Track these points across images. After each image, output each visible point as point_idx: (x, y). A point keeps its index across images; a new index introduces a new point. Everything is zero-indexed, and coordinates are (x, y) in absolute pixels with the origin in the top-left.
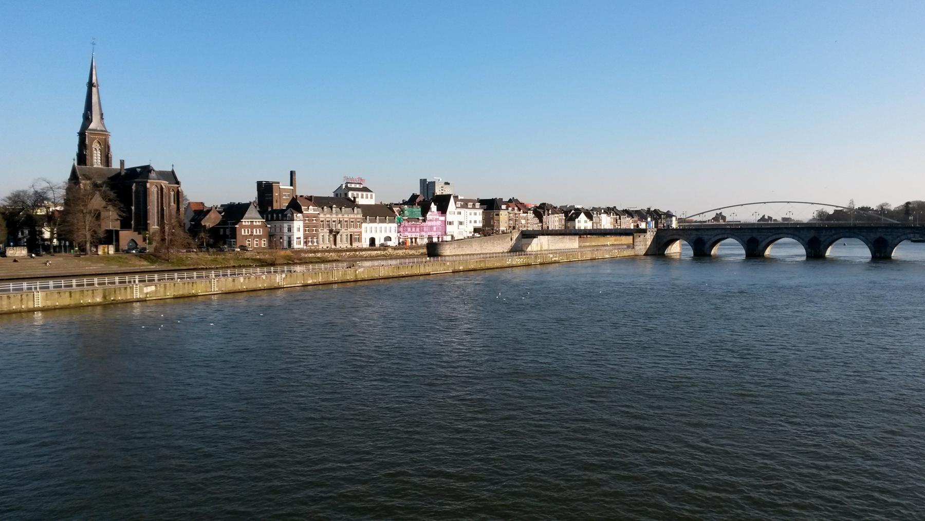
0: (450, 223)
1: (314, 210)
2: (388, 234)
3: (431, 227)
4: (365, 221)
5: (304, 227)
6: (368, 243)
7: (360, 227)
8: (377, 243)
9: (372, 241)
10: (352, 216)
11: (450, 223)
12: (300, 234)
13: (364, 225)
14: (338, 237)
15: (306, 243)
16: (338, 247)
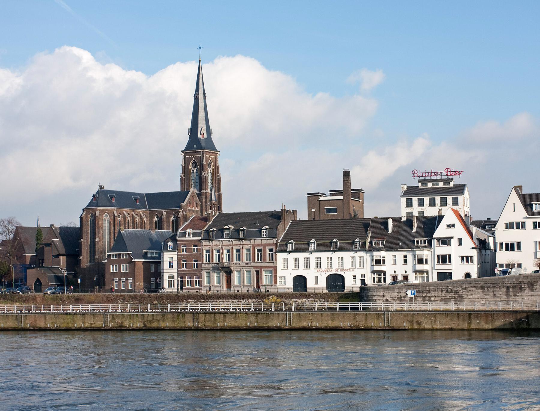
0: (510, 247)
1: (194, 235)
2: (336, 269)
3: (444, 259)
4: (284, 249)
5: (179, 260)
6: (290, 284)
7: (273, 258)
8: (310, 284)
9: (300, 282)
10: (258, 242)
11: (510, 247)
12: (174, 271)
13: (280, 256)
14: (235, 276)
15: (182, 285)
16: (233, 291)
